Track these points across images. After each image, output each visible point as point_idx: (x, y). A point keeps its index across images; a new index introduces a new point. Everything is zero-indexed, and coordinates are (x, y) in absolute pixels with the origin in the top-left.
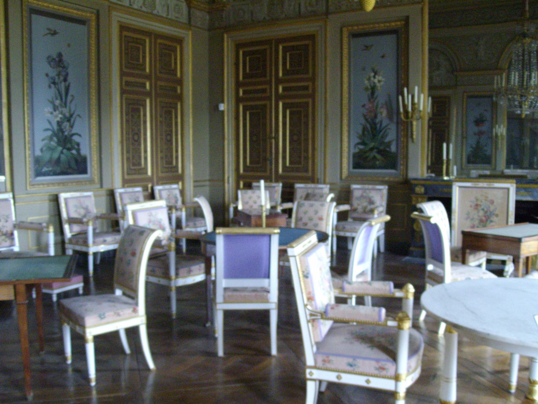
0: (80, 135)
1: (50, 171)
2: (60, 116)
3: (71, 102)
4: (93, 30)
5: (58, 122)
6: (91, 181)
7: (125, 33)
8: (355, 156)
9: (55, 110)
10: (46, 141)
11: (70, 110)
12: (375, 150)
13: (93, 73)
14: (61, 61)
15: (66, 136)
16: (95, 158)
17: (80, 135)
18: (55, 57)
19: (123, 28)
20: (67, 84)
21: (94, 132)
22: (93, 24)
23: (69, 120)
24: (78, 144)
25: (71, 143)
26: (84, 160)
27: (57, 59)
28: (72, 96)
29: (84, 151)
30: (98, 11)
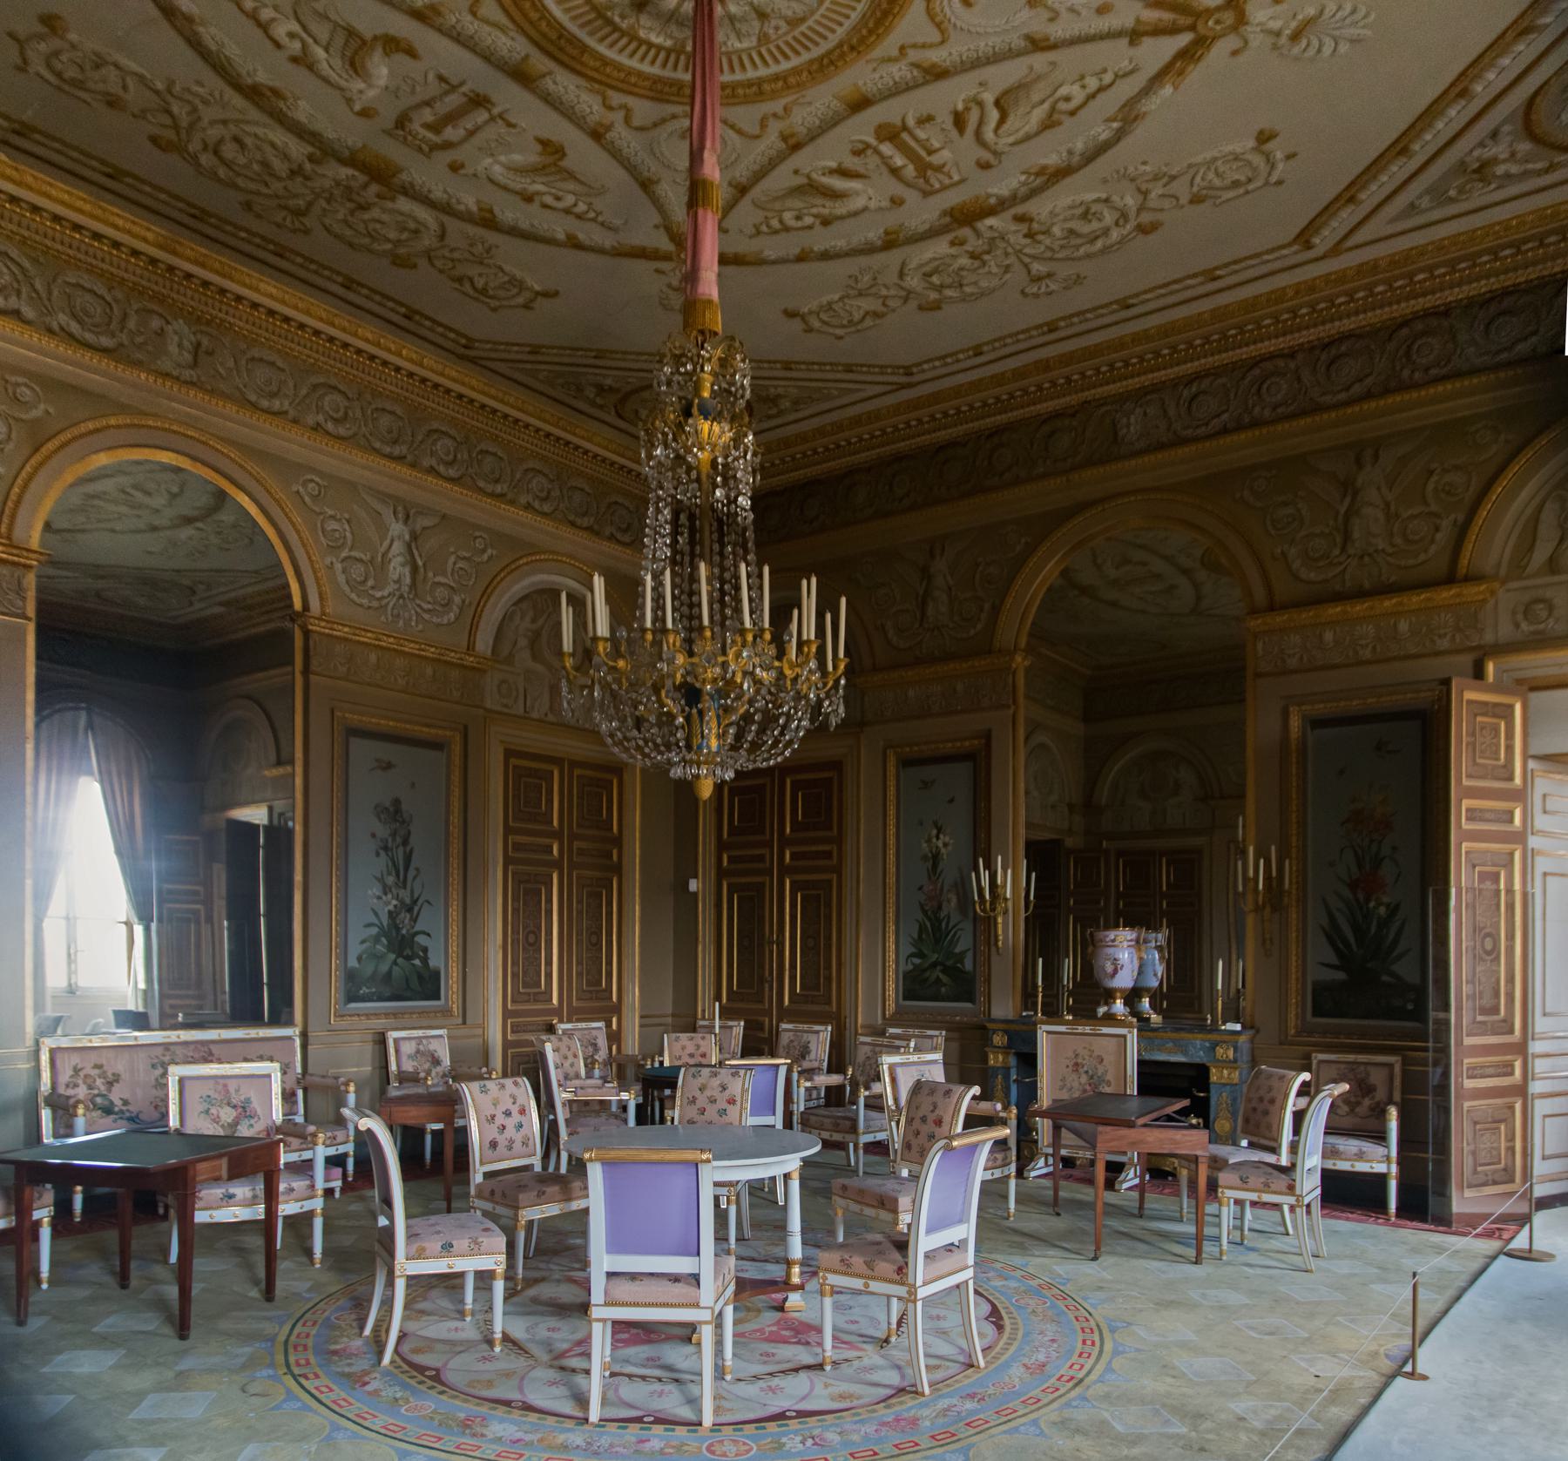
0: (429, 935)
1: (373, 993)
2: (394, 902)
3: (415, 878)
4: (457, 760)
5: (390, 912)
6: (446, 1012)
7: (513, 761)
8: (906, 975)
9: (386, 894)
10: (367, 944)
11: (412, 892)
12: (939, 968)
13: (456, 831)
14: (398, 811)
15: (403, 936)
16: (455, 972)
17: (429, 935)
18: (387, 804)
19: (509, 753)
20: (408, 849)
21: (455, 930)
22: (457, 749)
23: (410, 910)
24: (425, 950)
25: (412, 948)
26: (436, 975)
27: (391, 809)
28: (417, 869)
29: (435, 961)
30: (466, 727)
